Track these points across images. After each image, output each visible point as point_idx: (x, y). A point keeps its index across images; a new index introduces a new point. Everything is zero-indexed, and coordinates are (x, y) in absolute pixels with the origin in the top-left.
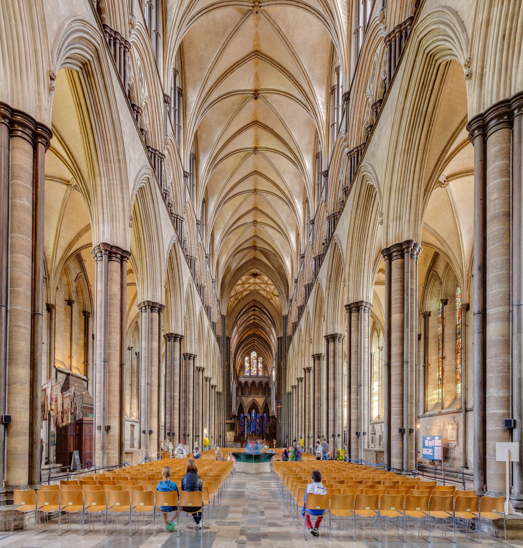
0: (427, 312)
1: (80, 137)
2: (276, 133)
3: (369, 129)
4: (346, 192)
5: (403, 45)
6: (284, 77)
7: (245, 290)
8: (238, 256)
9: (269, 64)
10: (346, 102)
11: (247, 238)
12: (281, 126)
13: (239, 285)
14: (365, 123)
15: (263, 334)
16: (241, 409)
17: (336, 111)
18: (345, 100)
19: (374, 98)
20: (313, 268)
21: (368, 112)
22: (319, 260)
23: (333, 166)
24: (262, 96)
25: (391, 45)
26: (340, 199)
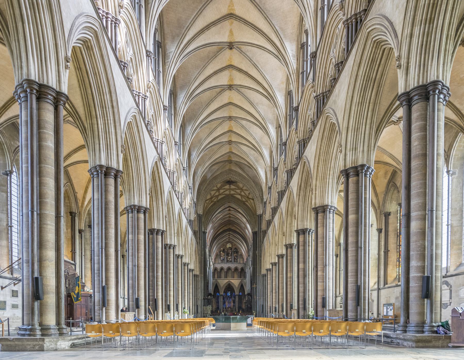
0: (387, 212)
1: (78, 89)
2: (250, 75)
3: (333, 81)
4: (314, 124)
5: (359, 28)
7: (220, 195)
8: (214, 167)
10: (313, 59)
11: (222, 154)
12: (255, 70)
13: (214, 190)
14: (329, 76)
15: (238, 228)
16: (216, 288)
17: (305, 62)
19: (337, 60)
20: (286, 179)
21: (332, 68)
22: (291, 173)
23: (303, 104)
24: (237, 47)
25: (348, 28)
26: (309, 129)
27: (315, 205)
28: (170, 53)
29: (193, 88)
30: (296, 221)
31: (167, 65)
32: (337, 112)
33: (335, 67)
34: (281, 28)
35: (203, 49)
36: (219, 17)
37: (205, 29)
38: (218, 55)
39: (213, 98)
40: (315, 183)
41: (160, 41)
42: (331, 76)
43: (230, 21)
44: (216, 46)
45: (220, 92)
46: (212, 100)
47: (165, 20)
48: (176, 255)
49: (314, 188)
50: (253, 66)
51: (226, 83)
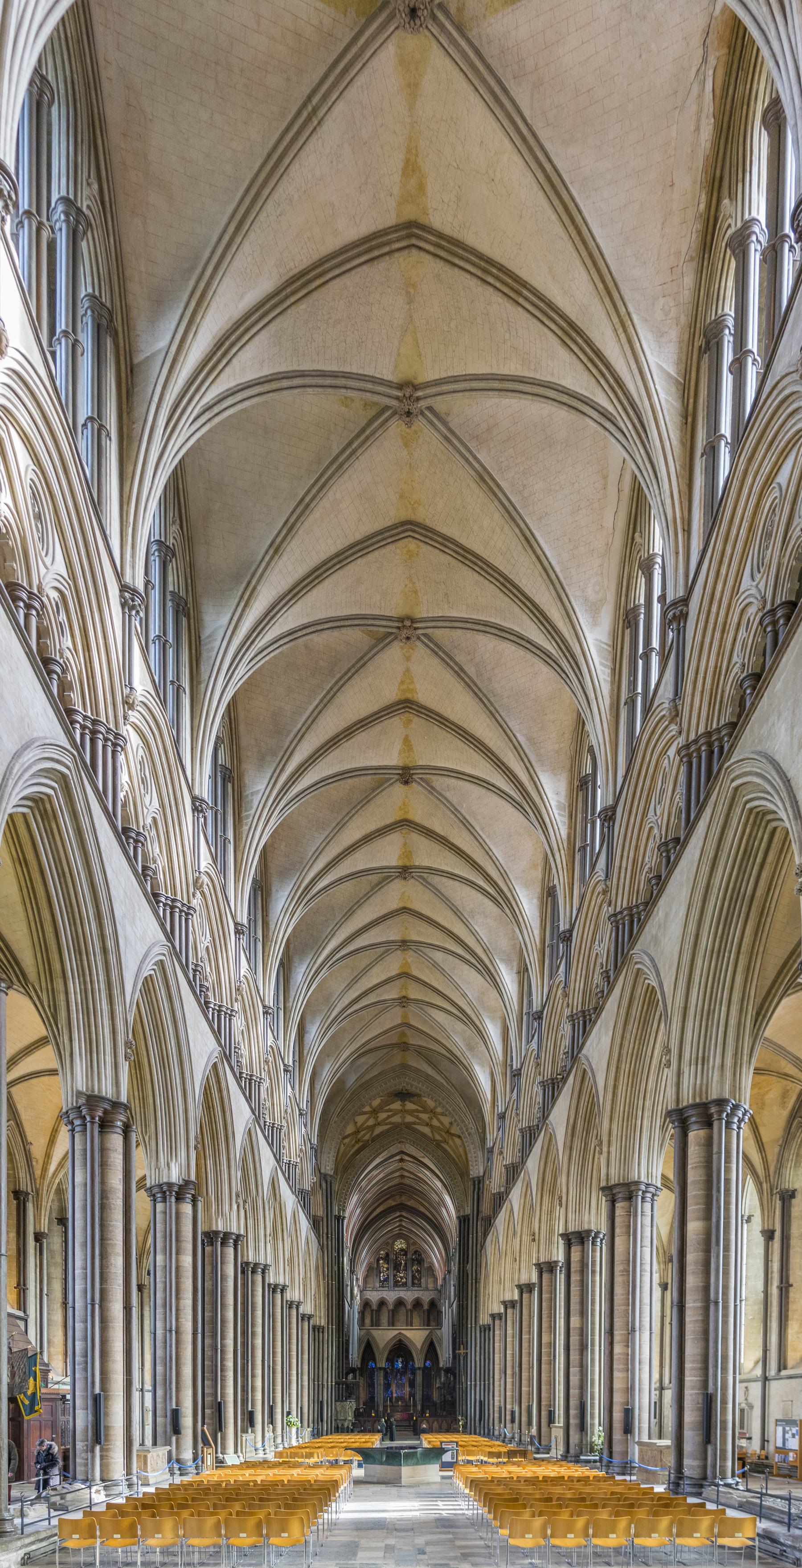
6: (472, 751)
9: (436, 727)
18: (605, 820)
19: (663, 833)
27: (607, 1180)
28: (252, 794)
29: (312, 874)
30: (563, 1210)
31: (246, 824)
32: (660, 966)
33: (659, 850)
34: (529, 739)
35: (334, 784)
36: (376, 708)
37: (340, 737)
38: (374, 797)
39: (361, 898)
40: (608, 1126)
41: (228, 765)
42: (651, 869)
43: (404, 717)
44: (369, 777)
45: (380, 883)
46: (358, 902)
47: (242, 715)
48: (269, 1285)
49: (605, 1139)
50: (461, 825)
51: (394, 862)
